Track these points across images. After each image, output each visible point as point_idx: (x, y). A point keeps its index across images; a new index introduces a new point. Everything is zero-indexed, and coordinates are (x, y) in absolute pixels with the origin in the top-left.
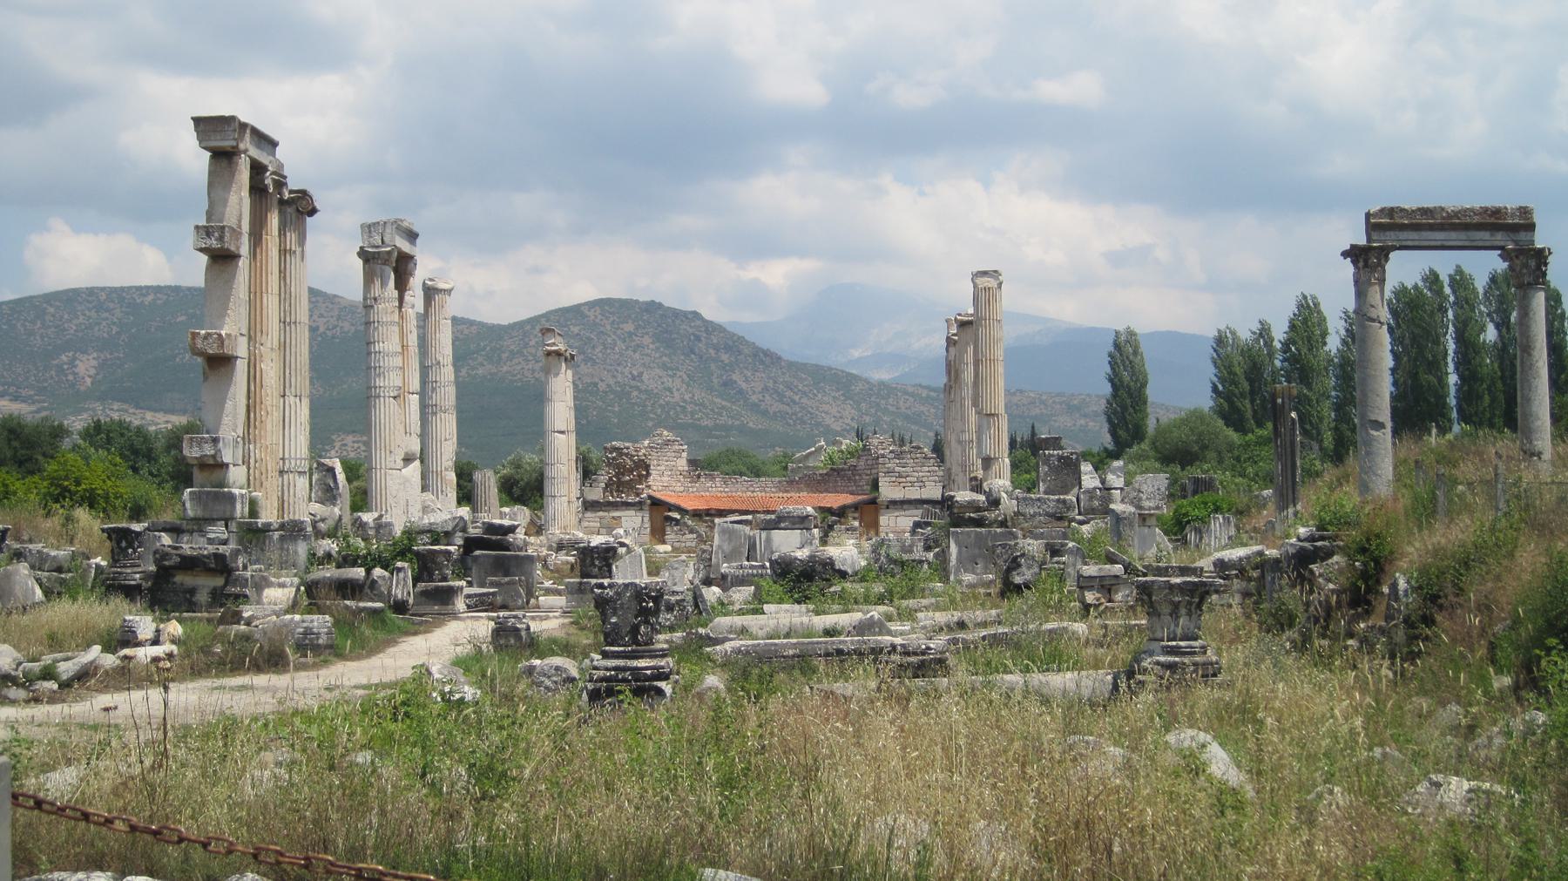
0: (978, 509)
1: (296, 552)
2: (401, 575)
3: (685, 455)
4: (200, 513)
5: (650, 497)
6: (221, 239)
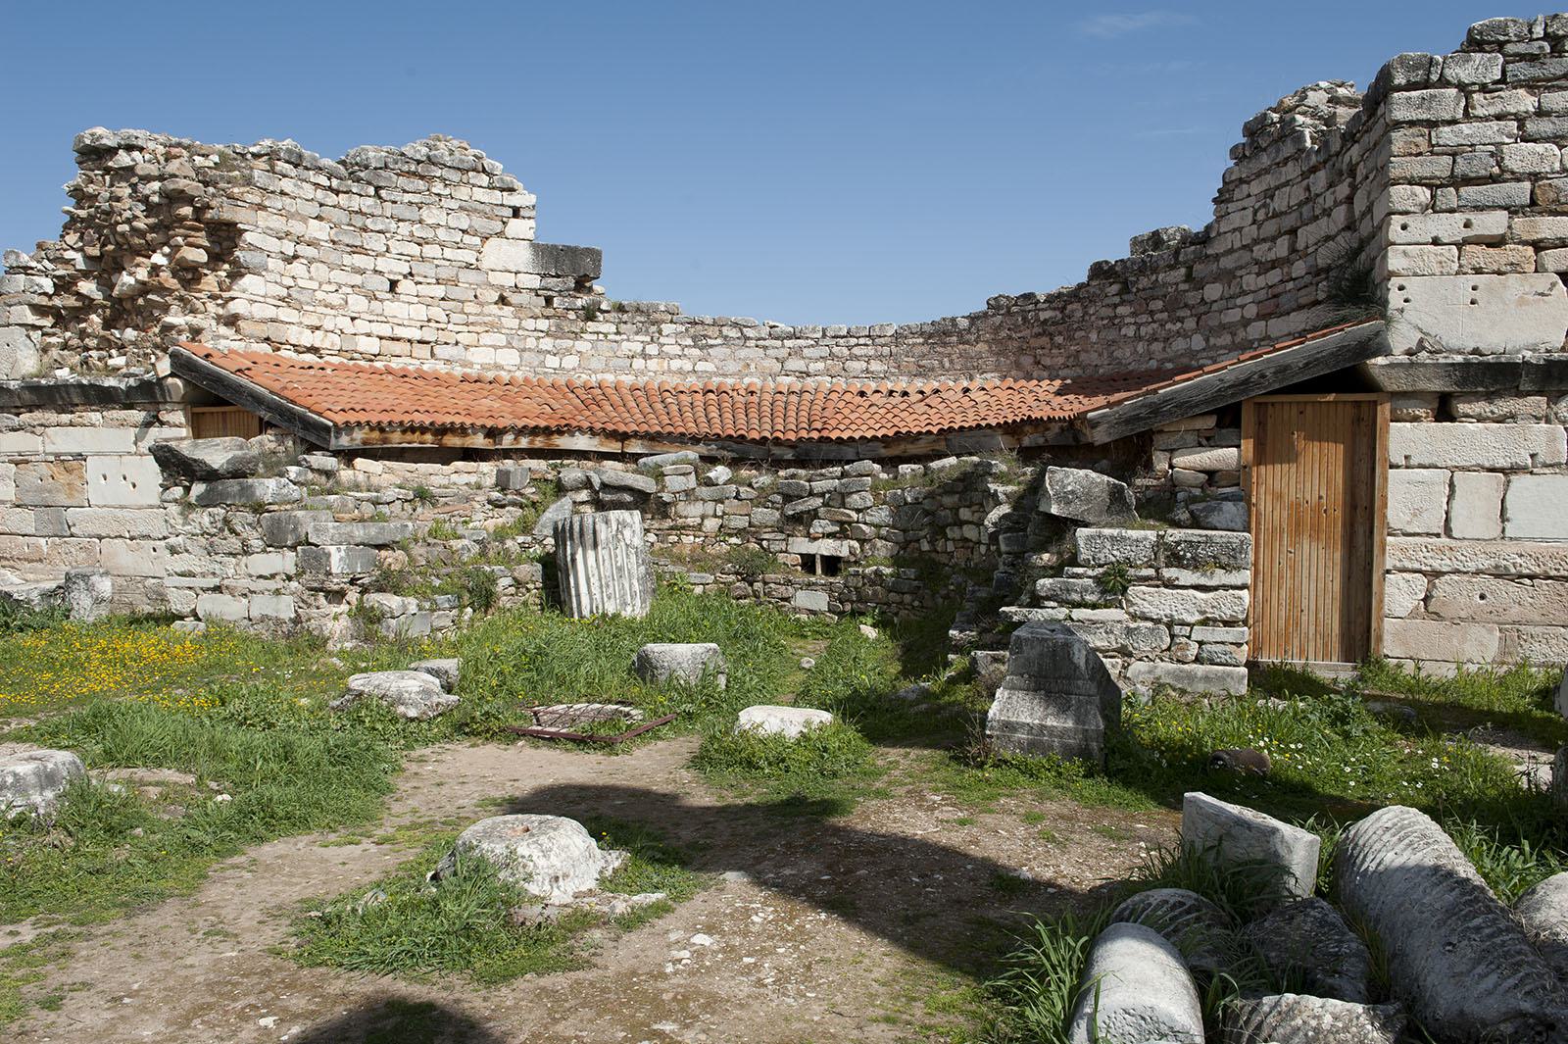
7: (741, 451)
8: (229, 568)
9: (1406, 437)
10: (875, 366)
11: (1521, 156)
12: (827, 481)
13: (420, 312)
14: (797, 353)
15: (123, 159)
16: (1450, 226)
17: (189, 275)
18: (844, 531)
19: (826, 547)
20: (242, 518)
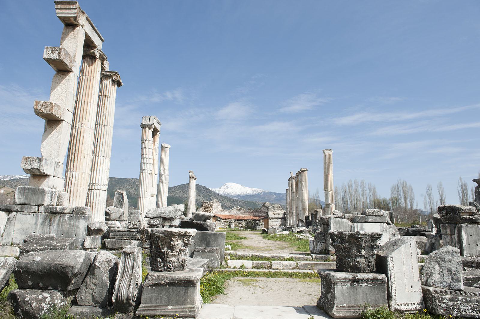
0: (472, 214)
1: (78, 227)
2: (130, 262)
3: (220, 205)
4: (22, 201)
6: (59, 54)
7: (235, 220)
8: (220, 225)
9: (270, 220)
12: (241, 222)
15: (207, 203)
17: (210, 209)
18: (242, 224)
19: (241, 225)
20: (221, 223)
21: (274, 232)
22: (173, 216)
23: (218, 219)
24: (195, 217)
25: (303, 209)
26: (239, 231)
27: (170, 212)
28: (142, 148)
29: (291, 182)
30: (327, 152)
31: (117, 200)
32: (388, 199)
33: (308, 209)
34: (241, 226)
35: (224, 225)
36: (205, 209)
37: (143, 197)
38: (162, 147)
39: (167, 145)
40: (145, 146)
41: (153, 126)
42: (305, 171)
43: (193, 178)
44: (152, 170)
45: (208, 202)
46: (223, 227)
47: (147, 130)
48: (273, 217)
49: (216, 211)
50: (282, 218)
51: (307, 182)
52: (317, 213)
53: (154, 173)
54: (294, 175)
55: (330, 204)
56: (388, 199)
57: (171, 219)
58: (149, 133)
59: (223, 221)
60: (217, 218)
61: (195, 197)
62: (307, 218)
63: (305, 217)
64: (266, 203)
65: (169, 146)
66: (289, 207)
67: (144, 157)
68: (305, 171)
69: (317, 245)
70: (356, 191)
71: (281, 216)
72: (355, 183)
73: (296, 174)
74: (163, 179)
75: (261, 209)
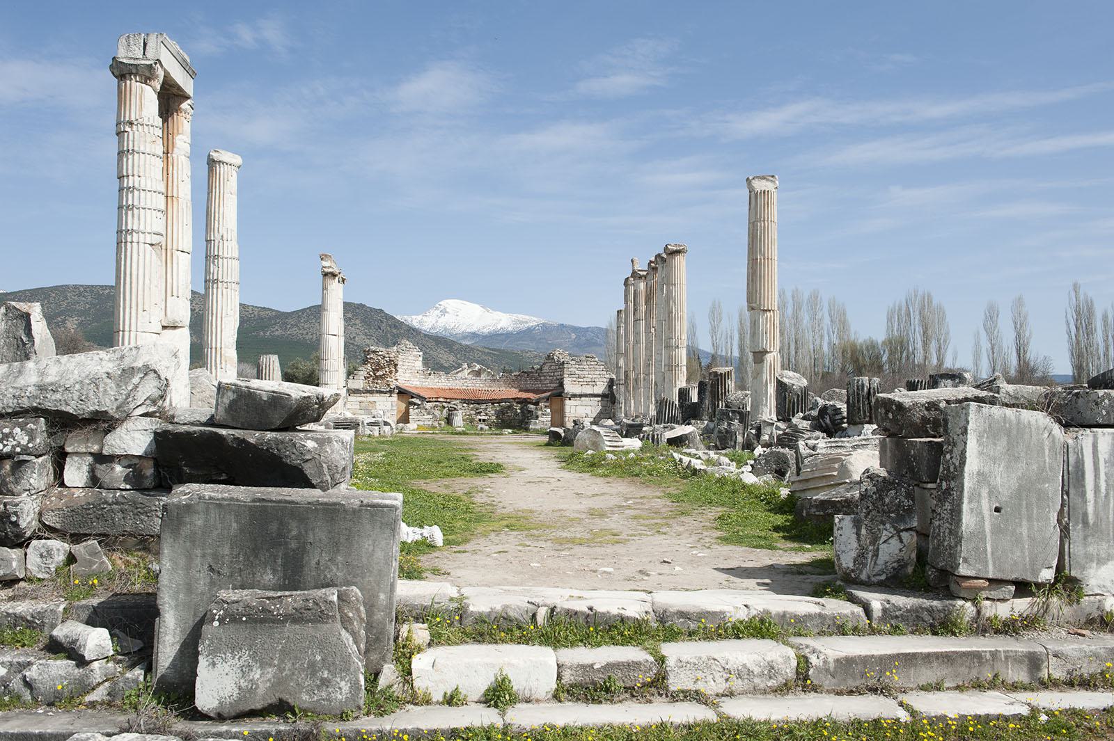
3: (421, 359)
5: (398, 387)
7: (468, 402)
8: (421, 418)
9: (567, 402)
10: (481, 385)
11: (577, 372)
12: (483, 406)
13: (408, 375)
14: (466, 382)
15: (380, 353)
16: (570, 379)
17: (391, 372)
18: (486, 415)
19: (483, 418)
20: (423, 411)
21: (596, 445)
22: (108, 405)
23: (413, 400)
24: (232, 407)
25: (671, 367)
26: (478, 434)
27: (95, 381)
28: (121, 153)
29: (632, 289)
30: (759, 185)
31: (8, 337)
32: (880, 342)
33: (684, 369)
34: (484, 420)
35: (431, 417)
36: (375, 370)
37: (133, 328)
38: (212, 163)
39: (229, 154)
40: (131, 143)
41: (161, 73)
42: (678, 252)
43: (334, 275)
44: (164, 234)
45: (383, 350)
46: (430, 423)
47: (135, 85)
48: (577, 390)
49: (407, 375)
50: (603, 396)
51: (685, 287)
52: (719, 380)
53: (175, 247)
54: (642, 266)
55: (765, 352)
56: (880, 342)
57: (102, 422)
58: (146, 99)
59: (428, 405)
60: (412, 397)
61: (342, 333)
62: (683, 394)
63: (676, 391)
64: (557, 353)
65: (238, 160)
66: (626, 364)
67: (131, 185)
68: (678, 252)
69: (875, 540)
70: (797, 320)
71: (600, 388)
72: (793, 297)
73: (649, 264)
74: (220, 272)
75: (541, 369)
